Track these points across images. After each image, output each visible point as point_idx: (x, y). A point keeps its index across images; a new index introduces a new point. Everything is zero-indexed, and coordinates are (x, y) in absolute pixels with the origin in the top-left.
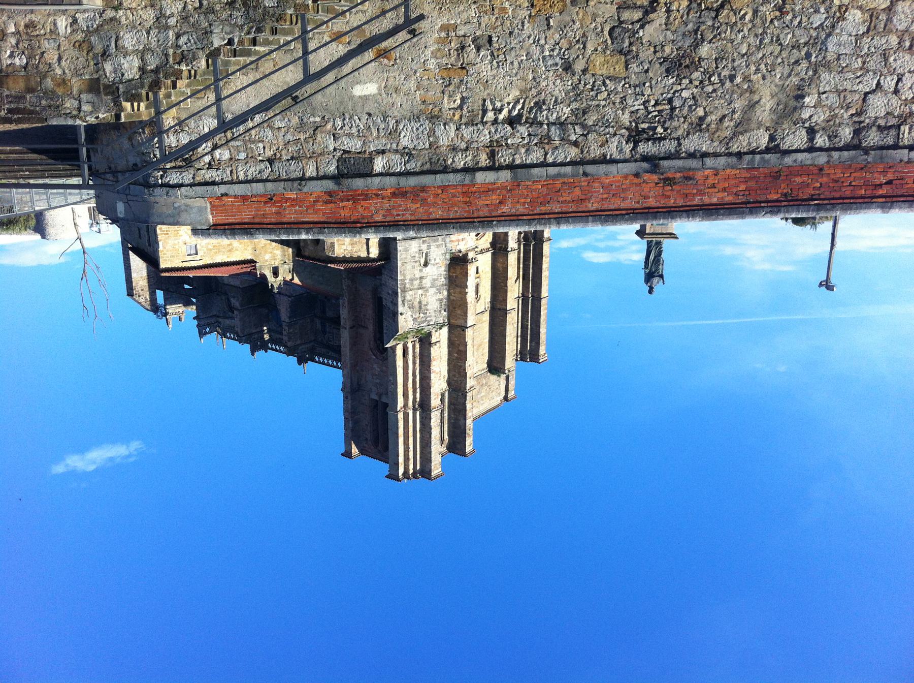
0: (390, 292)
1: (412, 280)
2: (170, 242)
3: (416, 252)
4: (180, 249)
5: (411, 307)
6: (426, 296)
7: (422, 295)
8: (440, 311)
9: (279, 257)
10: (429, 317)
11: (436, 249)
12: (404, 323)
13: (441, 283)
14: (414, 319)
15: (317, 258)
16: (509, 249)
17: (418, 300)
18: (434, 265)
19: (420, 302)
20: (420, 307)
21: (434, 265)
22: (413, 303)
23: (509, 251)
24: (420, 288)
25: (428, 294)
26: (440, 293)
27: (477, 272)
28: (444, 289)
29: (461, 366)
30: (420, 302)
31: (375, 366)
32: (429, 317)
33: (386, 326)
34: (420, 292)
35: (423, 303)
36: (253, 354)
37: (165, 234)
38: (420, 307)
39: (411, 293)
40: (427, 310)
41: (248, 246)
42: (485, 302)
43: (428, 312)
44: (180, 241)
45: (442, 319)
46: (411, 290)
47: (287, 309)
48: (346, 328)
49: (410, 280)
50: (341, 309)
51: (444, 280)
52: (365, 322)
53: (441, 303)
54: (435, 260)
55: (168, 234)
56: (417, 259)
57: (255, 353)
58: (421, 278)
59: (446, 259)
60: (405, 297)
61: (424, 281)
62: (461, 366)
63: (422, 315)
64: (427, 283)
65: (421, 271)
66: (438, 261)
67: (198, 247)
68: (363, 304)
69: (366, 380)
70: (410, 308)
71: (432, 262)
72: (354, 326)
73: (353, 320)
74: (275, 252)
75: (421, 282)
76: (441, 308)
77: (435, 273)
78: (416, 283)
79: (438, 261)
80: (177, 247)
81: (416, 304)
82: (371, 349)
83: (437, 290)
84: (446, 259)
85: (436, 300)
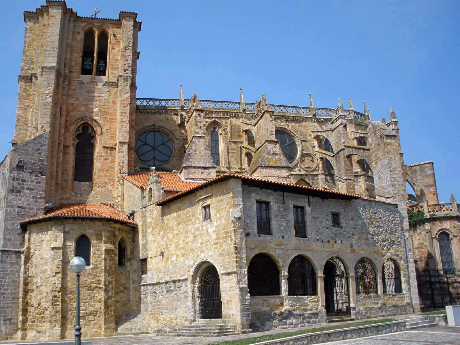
0: (27, 191)
2: (224, 222)
4: (215, 212)
15: (79, 221)
33: (40, 154)
47: (195, 151)
48: (120, 142)
50: (126, 162)
52: (107, 153)
68: (107, 171)
80: (218, 216)
82: (99, 125)
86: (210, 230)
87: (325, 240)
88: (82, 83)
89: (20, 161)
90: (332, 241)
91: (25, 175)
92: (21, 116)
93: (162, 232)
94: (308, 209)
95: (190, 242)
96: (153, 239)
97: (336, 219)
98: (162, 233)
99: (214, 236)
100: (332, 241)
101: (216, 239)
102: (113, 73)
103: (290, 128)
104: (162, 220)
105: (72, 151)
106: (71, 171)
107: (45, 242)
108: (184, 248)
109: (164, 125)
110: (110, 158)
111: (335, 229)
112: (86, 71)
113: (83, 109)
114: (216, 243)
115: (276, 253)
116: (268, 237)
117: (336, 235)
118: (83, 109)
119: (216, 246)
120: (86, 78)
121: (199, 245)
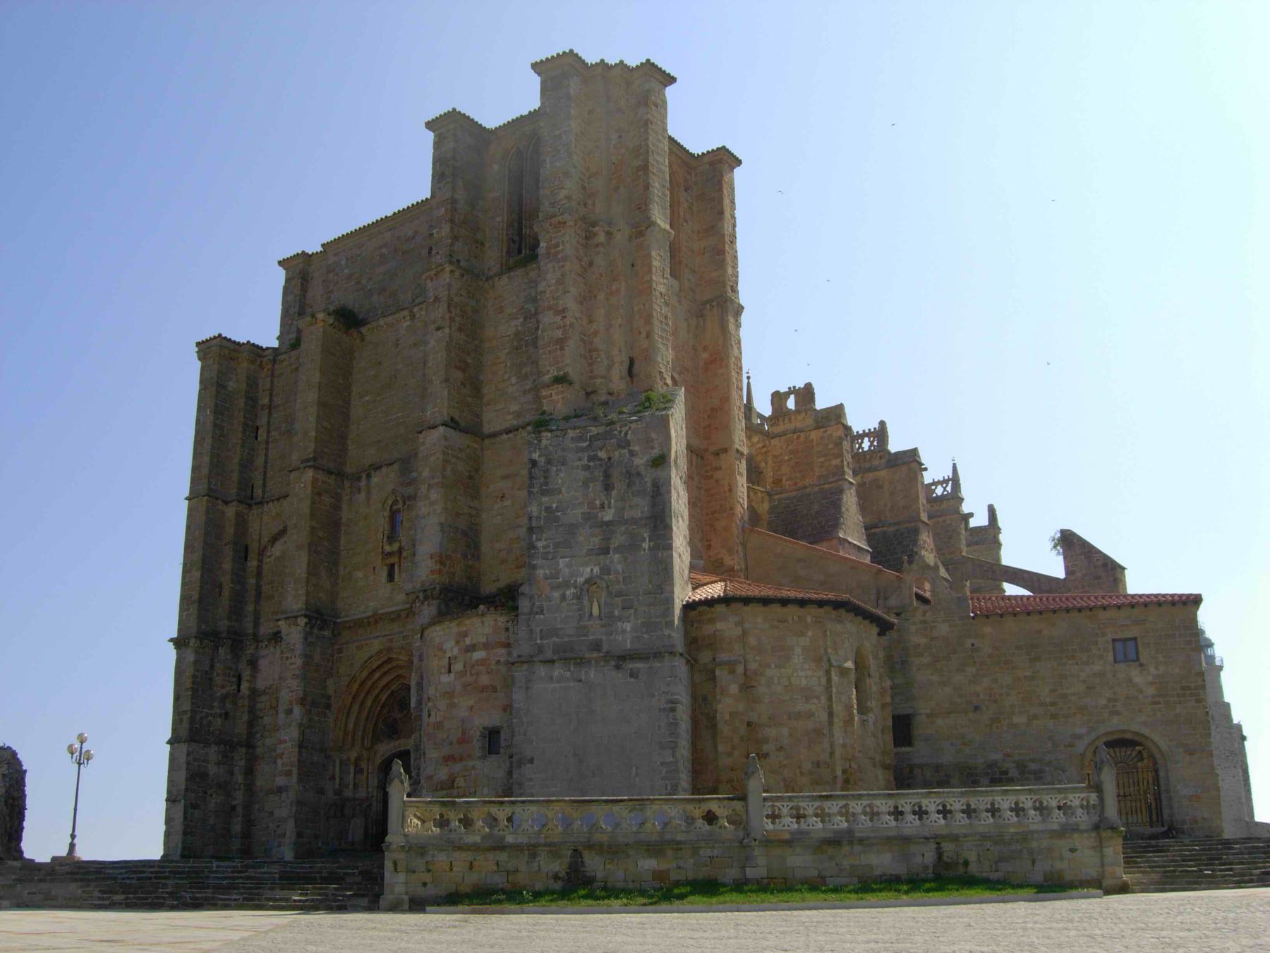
1: (633, 546)
2: (1177, 670)
3: (620, 619)
5: (631, 476)
6: (591, 504)
7: (602, 506)
8: (549, 462)
9: (913, 628)
10: (582, 450)
11: (559, 626)
12: (654, 435)
13: (544, 536)
14: (624, 444)
16: (302, 621)
17: (614, 493)
18: (566, 585)
19: (608, 488)
20: (607, 476)
21: (566, 585)
22: (629, 485)
23: (305, 616)
24: (608, 524)
25: (585, 509)
26: (548, 509)
27: (391, 568)
28: (538, 518)
29: (460, 330)
30: (608, 488)
32: (582, 450)
34: (608, 516)
35: (599, 486)
36: (882, 424)
37: (1189, 688)
38: (607, 476)
39: (637, 514)
40: (587, 468)
41: (990, 656)
42: (369, 493)
43: (585, 461)
44: (1152, 670)
45: (544, 442)
46: (634, 521)
47: (847, 510)
49: (641, 546)
51: (539, 544)
53: (546, 484)
54: (563, 597)
55: (1183, 688)
56: (618, 600)
57: (877, 426)
58: (605, 551)
59: (531, 597)
60: (654, 505)
61: (596, 541)
62: (460, 330)
63: (602, 454)
64: (588, 539)
65: (606, 570)
66: (556, 594)
67: (1110, 657)
69: (688, 325)
70: (639, 474)
71: (573, 590)
72: (717, 454)
73: (718, 468)
74: (923, 641)
75: (607, 539)
76: (547, 471)
77: (562, 563)
78: (619, 539)
79: (556, 594)
80: (1161, 658)
81: (619, 486)
83: (556, 519)
84: (531, 597)
85: (560, 492)
86: (1138, 679)
92: (576, 319)
93: (974, 669)
95: (1074, 694)
96: (935, 678)
98: (971, 670)
99: (1151, 691)
101: (1153, 696)
102: (689, 280)
104: (973, 645)
107: (798, 650)
108: (1053, 704)
110: (696, 479)
114: (1159, 703)
119: (1156, 706)
121: (1103, 702)
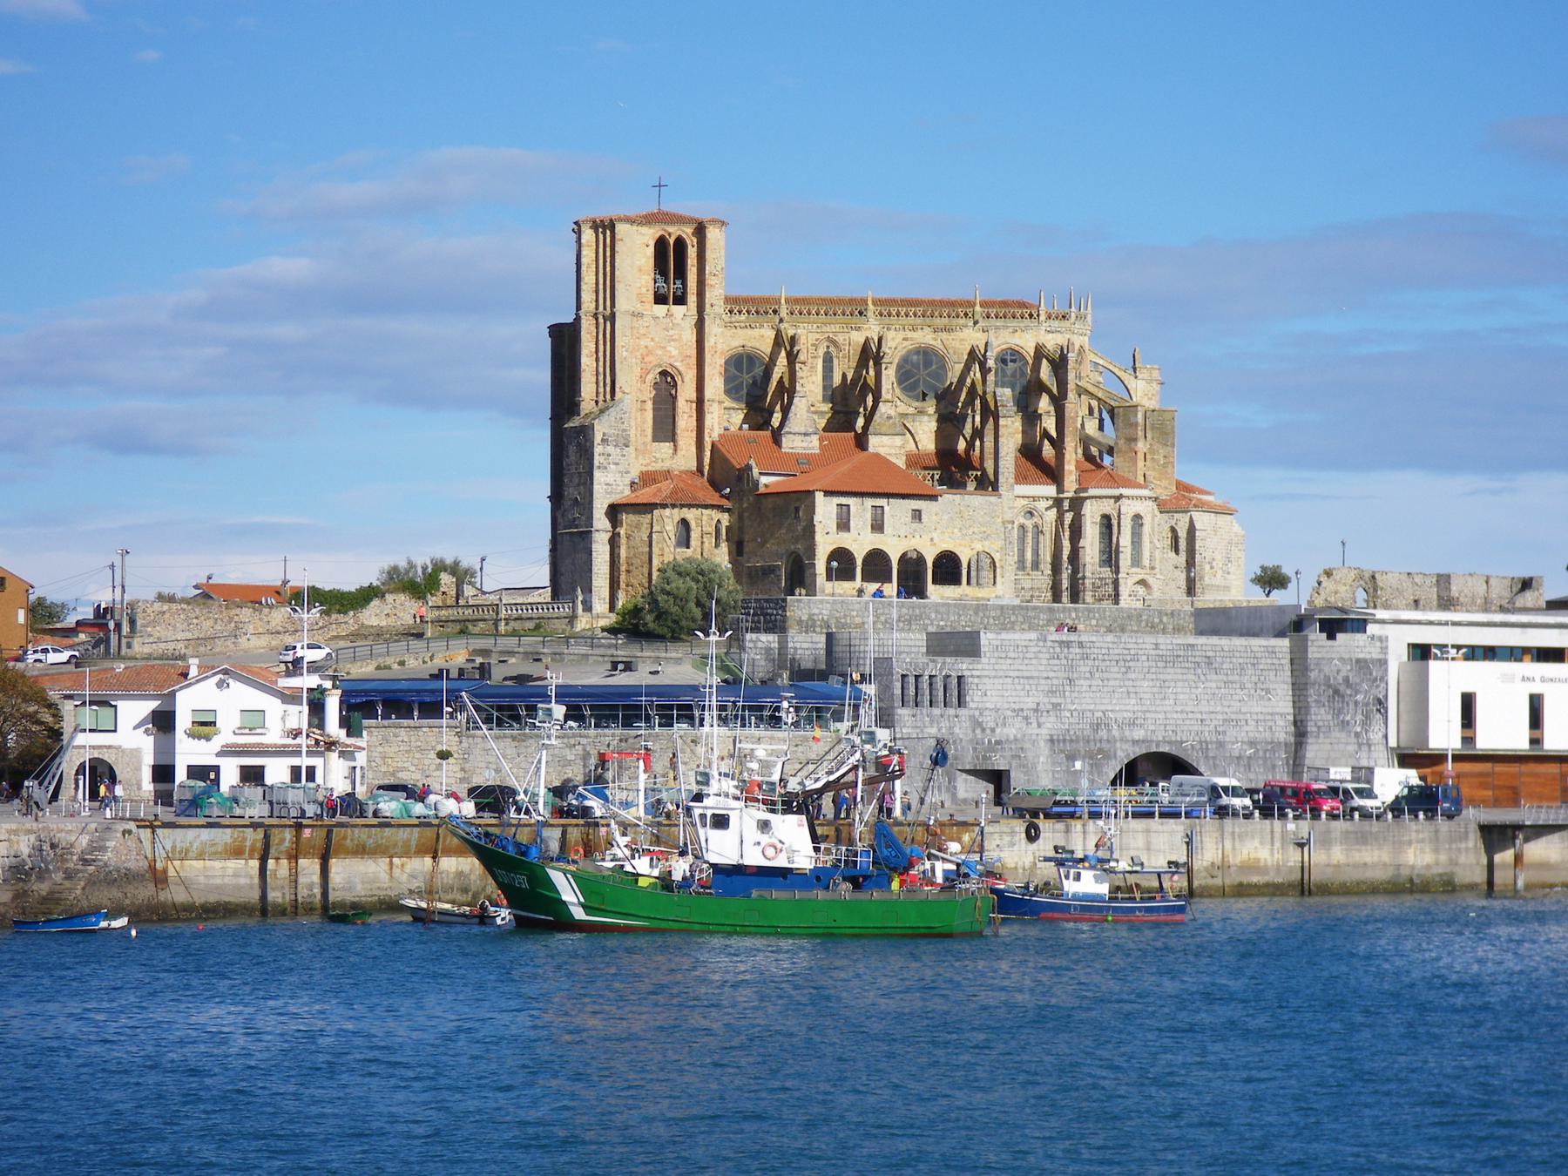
0: (612, 466)
31: (675, 352)
87: (902, 535)
88: (656, 318)
89: (604, 434)
90: (910, 536)
91: (610, 449)
94: (887, 509)
97: (917, 515)
100: (910, 536)
103: (938, 344)
105: (649, 406)
106: (649, 432)
109: (757, 345)
111: (915, 525)
112: (660, 299)
113: (660, 352)
115: (853, 548)
116: (845, 535)
117: (915, 530)
118: (660, 352)
120: (661, 309)
